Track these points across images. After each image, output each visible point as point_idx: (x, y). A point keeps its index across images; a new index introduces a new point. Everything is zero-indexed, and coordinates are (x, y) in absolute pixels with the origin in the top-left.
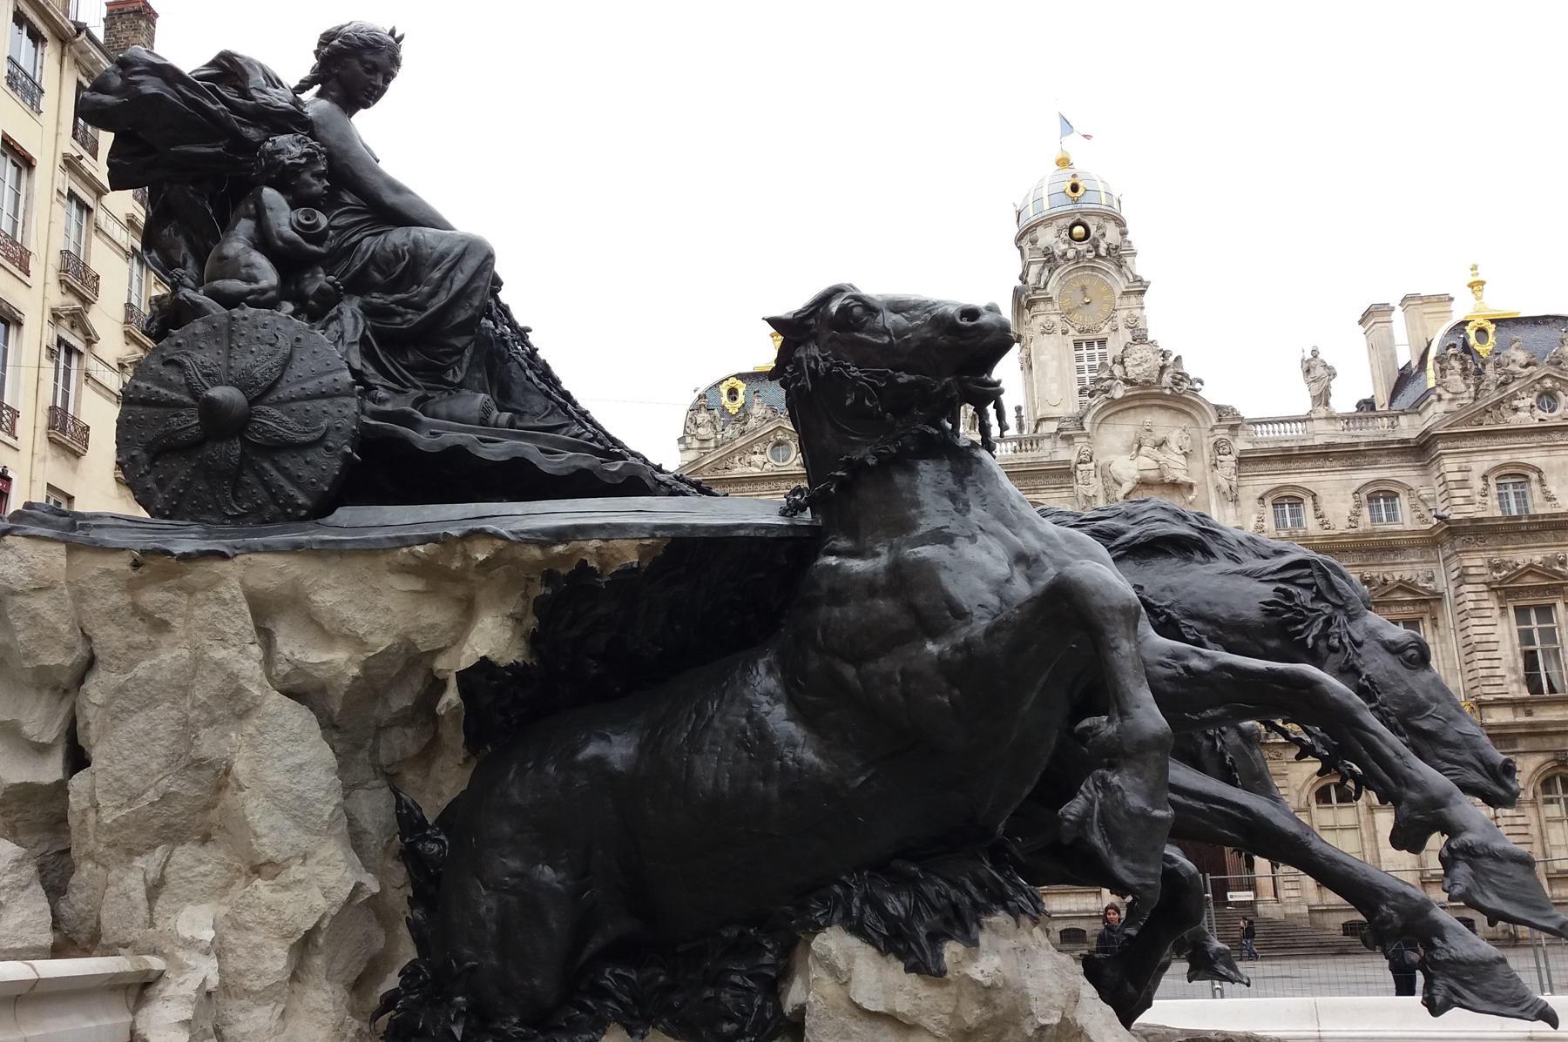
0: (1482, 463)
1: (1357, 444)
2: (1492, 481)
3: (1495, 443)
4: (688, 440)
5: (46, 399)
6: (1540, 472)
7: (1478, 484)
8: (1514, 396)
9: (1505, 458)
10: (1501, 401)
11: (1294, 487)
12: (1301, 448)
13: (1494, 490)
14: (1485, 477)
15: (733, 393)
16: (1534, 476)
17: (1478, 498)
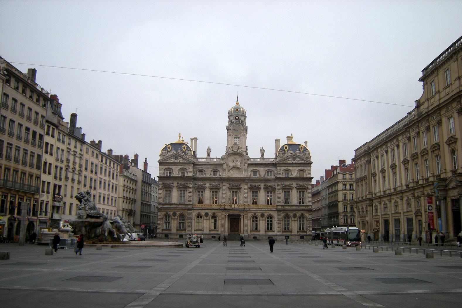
0: (283, 168)
1: (266, 163)
2: (284, 171)
3: (285, 165)
4: (161, 155)
5: (65, 175)
6: (291, 170)
7: (282, 172)
8: (289, 158)
9: (286, 168)
10: (287, 159)
11: (256, 170)
12: (258, 163)
13: (284, 172)
14: (283, 171)
15: (169, 148)
16: (290, 171)
17: (282, 174)
